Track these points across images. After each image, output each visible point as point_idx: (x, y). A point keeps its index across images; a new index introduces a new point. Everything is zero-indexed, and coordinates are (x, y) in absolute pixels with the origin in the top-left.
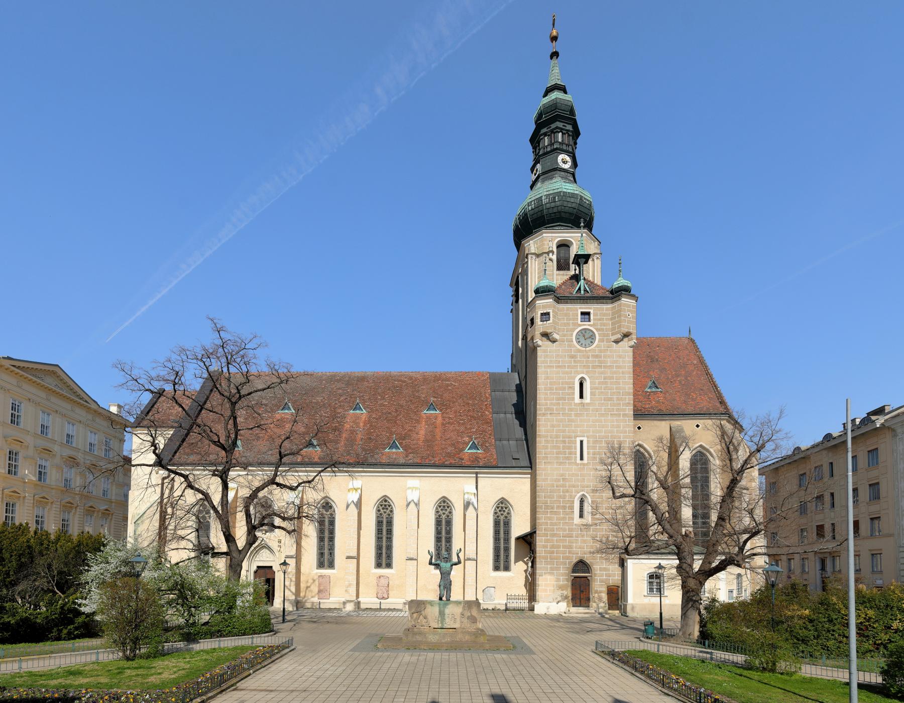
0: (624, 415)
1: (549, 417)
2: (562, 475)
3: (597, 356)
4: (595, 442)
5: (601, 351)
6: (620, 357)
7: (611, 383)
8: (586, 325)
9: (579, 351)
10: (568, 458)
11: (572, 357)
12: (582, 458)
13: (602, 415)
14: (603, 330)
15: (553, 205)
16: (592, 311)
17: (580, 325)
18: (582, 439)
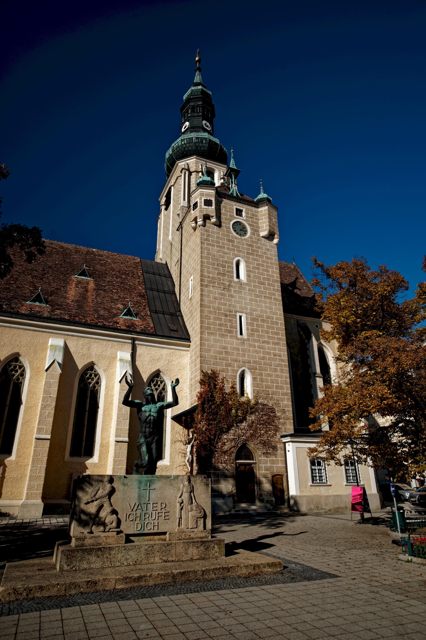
0: (275, 299)
1: (211, 289)
2: (224, 348)
3: (250, 245)
4: (253, 319)
5: (253, 242)
6: (268, 250)
9: (236, 238)
10: (230, 332)
11: (229, 241)
13: (258, 296)
14: (253, 226)
15: (201, 145)
16: (244, 210)
17: (236, 218)
18: (241, 314)
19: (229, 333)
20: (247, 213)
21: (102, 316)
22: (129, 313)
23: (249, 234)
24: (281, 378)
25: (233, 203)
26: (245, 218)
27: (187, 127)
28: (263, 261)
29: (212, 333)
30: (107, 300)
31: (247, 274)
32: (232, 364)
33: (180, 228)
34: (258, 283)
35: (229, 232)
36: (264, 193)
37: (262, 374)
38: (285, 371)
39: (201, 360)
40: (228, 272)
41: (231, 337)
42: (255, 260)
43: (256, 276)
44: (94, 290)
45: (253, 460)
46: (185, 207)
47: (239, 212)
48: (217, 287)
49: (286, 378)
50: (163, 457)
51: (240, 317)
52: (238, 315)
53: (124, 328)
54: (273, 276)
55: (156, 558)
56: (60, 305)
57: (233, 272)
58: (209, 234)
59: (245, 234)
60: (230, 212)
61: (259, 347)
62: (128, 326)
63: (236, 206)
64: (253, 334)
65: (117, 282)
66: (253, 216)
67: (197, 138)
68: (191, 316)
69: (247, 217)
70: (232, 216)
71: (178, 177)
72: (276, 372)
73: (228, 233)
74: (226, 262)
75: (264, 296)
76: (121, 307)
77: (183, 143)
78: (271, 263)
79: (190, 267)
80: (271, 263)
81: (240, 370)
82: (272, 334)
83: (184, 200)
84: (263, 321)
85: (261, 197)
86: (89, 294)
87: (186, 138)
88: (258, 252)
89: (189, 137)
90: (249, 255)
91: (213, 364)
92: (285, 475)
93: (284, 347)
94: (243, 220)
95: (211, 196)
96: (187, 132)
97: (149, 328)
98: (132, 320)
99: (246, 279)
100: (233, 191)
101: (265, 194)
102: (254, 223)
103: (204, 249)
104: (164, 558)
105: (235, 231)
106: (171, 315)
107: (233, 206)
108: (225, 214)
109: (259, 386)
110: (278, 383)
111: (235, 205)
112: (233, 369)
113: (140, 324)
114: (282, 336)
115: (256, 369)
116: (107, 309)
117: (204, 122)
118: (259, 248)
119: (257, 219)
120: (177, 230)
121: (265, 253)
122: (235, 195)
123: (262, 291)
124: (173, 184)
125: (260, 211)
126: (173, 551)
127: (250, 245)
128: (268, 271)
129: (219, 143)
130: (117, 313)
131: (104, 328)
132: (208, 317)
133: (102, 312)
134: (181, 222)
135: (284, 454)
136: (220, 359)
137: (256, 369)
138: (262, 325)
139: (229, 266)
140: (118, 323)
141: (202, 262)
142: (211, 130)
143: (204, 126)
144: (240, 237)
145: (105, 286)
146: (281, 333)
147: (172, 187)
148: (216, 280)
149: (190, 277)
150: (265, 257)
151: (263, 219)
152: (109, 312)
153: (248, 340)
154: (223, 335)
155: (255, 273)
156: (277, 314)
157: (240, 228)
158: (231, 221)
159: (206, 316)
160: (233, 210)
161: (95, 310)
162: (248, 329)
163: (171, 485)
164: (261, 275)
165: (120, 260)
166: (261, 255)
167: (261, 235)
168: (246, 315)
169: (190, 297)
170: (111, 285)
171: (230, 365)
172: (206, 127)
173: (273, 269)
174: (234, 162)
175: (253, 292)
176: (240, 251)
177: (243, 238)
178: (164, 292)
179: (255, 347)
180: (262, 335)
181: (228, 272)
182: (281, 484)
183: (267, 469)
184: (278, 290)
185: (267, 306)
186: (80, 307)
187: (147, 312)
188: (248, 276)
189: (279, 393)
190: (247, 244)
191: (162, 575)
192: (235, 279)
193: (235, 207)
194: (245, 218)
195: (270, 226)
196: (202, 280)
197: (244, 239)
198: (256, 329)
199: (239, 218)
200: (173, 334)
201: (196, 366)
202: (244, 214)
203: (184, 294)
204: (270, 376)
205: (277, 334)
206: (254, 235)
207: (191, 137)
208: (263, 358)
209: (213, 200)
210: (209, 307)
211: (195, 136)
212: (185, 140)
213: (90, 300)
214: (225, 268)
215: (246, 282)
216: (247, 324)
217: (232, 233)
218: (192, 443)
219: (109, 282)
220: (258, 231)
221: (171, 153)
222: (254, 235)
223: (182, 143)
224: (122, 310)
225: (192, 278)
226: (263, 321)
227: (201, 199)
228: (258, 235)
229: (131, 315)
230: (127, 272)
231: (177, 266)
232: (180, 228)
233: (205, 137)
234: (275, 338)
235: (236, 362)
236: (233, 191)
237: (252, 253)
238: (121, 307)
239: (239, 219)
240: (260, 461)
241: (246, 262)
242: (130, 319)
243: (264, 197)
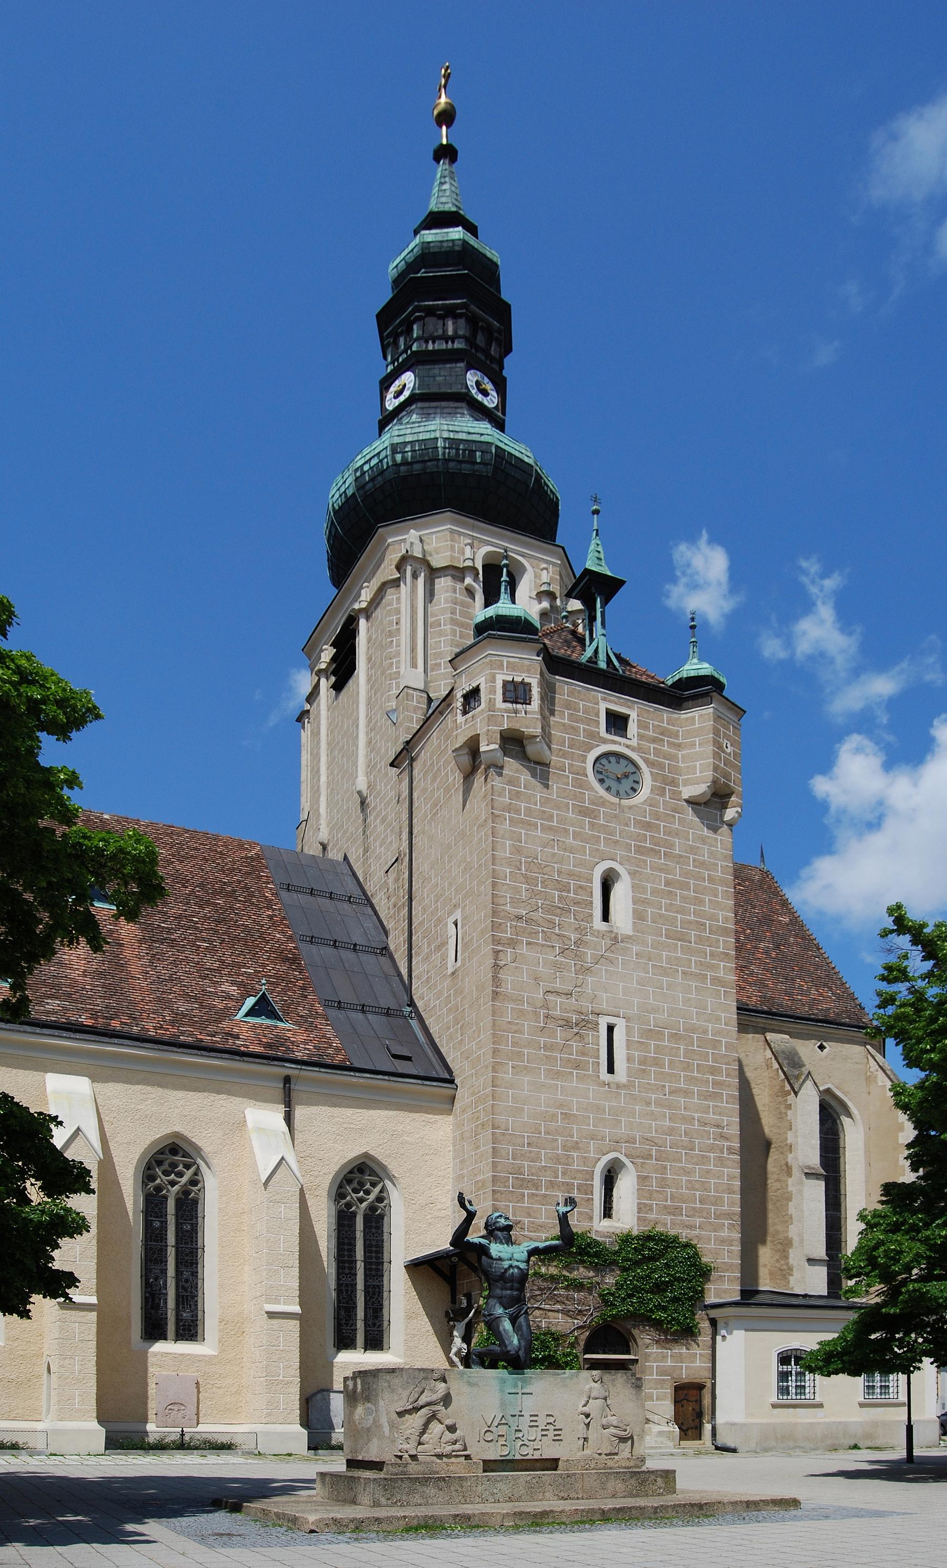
3: (648, 826)
5: (657, 816)
8: (617, 744)
9: (603, 803)
11: (584, 812)
12: (611, 1070)
14: (661, 766)
16: (633, 716)
17: (605, 741)
18: (612, 1020)
19: (577, 1067)
20: (642, 725)
23: (645, 792)
25: (598, 693)
26: (634, 742)
28: (686, 874)
29: (526, 1068)
31: (635, 911)
35: (581, 784)
36: (701, 660)
40: (577, 903)
42: (661, 870)
43: (661, 916)
47: (617, 723)
51: (611, 1029)
52: (603, 1022)
57: (592, 903)
59: (634, 790)
60: (589, 721)
63: (605, 701)
64: (644, 1070)
66: (662, 734)
69: (641, 737)
73: (581, 787)
74: (571, 874)
85: (693, 674)
88: (671, 846)
90: (642, 854)
91: (529, 1144)
94: (628, 746)
99: (630, 926)
100: (596, 651)
101: (706, 665)
105: (601, 781)
107: (598, 704)
108: (573, 727)
111: (604, 699)
119: (674, 744)
122: (603, 665)
125: (687, 719)
148: (539, 925)
150: (694, 861)
151: (693, 745)
154: (558, 1072)
157: (618, 773)
160: (597, 715)
162: (629, 1059)
171: (576, 1146)
175: (649, 959)
176: (617, 841)
177: (625, 802)
179: (648, 1104)
180: (670, 1075)
181: (577, 903)
188: (639, 916)
190: (637, 822)
192: (598, 923)
193: (603, 707)
194: (634, 742)
195: (716, 769)
198: (655, 1058)
199: (614, 742)
202: (632, 728)
208: (671, 1131)
214: (569, 892)
217: (591, 789)
236: (596, 651)
239: (617, 744)
241: (632, 874)
243: (702, 673)
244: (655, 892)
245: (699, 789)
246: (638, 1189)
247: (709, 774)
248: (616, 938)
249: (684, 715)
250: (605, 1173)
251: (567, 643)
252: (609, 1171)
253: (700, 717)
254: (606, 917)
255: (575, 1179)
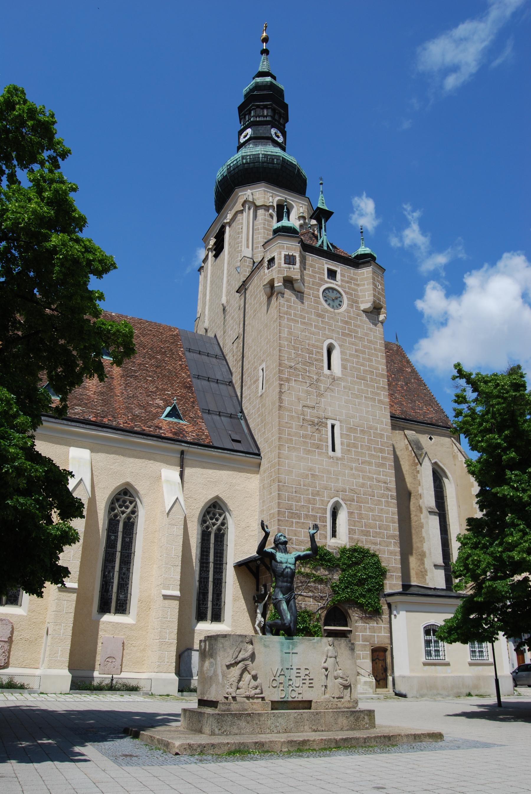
0: (380, 401)
1: (293, 384)
2: (310, 470)
3: (346, 323)
4: (350, 429)
7: (364, 359)
8: (332, 284)
9: (327, 311)
11: (319, 315)
12: (334, 450)
14: (351, 294)
16: (339, 271)
17: (327, 282)
18: (334, 422)
19: (318, 448)
20: (342, 275)
21: (138, 416)
22: (174, 413)
23: (345, 306)
24: (387, 513)
25: (324, 261)
26: (339, 283)
27: (248, 137)
28: (364, 346)
29: (294, 448)
30: (140, 393)
31: (342, 365)
32: (320, 493)
33: (242, 289)
34: (357, 378)
35: (318, 302)
36: (366, 246)
37: (361, 507)
38: (392, 505)
39: (279, 485)
40: (317, 360)
41: (320, 454)
42: (353, 344)
43: (354, 367)
44: (121, 377)
45: (346, 625)
46: (248, 258)
47: (332, 274)
48: (302, 382)
49: (393, 514)
50: (222, 620)
51: (333, 427)
52: (330, 423)
53: (170, 435)
54: (377, 369)
55: (306, 727)
56: (79, 399)
57: (323, 360)
58: (291, 305)
59: (340, 305)
60: (320, 273)
61: (357, 469)
62: (175, 434)
63: (327, 264)
64: (349, 450)
65: (152, 365)
66: (351, 279)
67: (266, 156)
68: (262, 421)
69: (342, 281)
70: (322, 280)
71: (237, 213)
72: (379, 505)
73: (317, 303)
74: (313, 346)
75: (365, 397)
76: (161, 403)
77: (244, 161)
78: (375, 349)
79: (261, 350)
80: (375, 349)
81: (332, 501)
82: (374, 451)
83: (248, 247)
84: (363, 432)
85: (363, 253)
86: (115, 382)
87: (249, 154)
89: (253, 153)
90: (344, 336)
91: (295, 492)
92: (389, 649)
93: (392, 470)
94: (337, 285)
95: (295, 250)
96: (249, 144)
97: (203, 437)
98: (179, 423)
99: (340, 372)
100: (323, 242)
101: (368, 249)
102: (352, 290)
103: (284, 327)
104: (314, 727)
105: (326, 301)
106: (231, 416)
107: (323, 265)
108: (313, 276)
109: (357, 524)
110: (381, 521)
111: (326, 263)
112: (322, 500)
113: (190, 429)
114: (388, 454)
115: (353, 500)
116: (144, 407)
117: (273, 131)
118: (359, 327)
120: (237, 292)
121: (367, 334)
122: (325, 248)
123: (362, 389)
124: (228, 221)
125: (361, 273)
126: (322, 721)
127: (346, 323)
128: (370, 360)
129: (295, 163)
130: (157, 413)
131: (142, 434)
132: (289, 425)
133: (137, 411)
134: (244, 282)
135: (388, 620)
136: (304, 485)
137: (353, 500)
138: (362, 438)
139: (318, 352)
140: (160, 428)
141: (280, 345)
142: (282, 142)
143: (274, 136)
144: (332, 310)
145: (135, 371)
146: (388, 450)
147: (227, 228)
148: (300, 371)
149: (260, 365)
150: (367, 340)
151: (364, 285)
152: (146, 412)
153: (342, 459)
154: (309, 450)
155: (353, 364)
156: (382, 422)
157: (333, 297)
158: (321, 285)
159: (286, 423)
160: (324, 270)
161: (127, 408)
162: (342, 444)
163: (315, 648)
164: (361, 365)
165: (150, 330)
166: (361, 338)
167: (362, 308)
168: (340, 423)
169: (260, 394)
170: (144, 370)
171: (318, 494)
172: (276, 138)
173: (378, 358)
174: (323, 199)
175: (350, 390)
176: (333, 330)
177: (336, 311)
178: (217, 381)
179: (352, 469)
180: (361, 452)
181: (317, 360)
182: (383, 660)
183: (365, 640)
184: (384, 388)
185: (368, 411)
186: (106, 402)
187: (197, 412)
188: (344, 367)
189: (384, 535)
190: (342, 320)
191: (325, 740)
192: (326, 371)
193: (326, 267)
194: (339, 283)
195: (374, 296)
196: (280, 371)
197: (339, 314)
198: (354, 443)
199: (331, 283)
200: (236, 446)
201: (271, 493)
202: (338, 276)
203: (249, 387)
204: (372, 510)
205: (382, 451)
206: (352, 307)
207: (256, 153)
208: (363, 485)
209: (297, 255)
210: (290, 411)
211: (263, 152)
212: (248, 157)
213: (118, 391)
214: (313, 354)
215: (341, 376)
216: (342, 435)
217: (322, 304)
218: (264, 602)
219: (140, 365)
220: (357, 302)
221: (225, 174)
222: (352, 307)
223: (242, 162)
224: (162, 409)
225: (264, 365)
226: (363, 432)
227: (280, 254)
228: (358, 308)
229: (178, 417)
230: (163, 350)
231: (235, 344)
232: (242, 289)
233: (277, 154)
234: (379, 457)
235: (326, 489)
236: (323, 242)
237: (349, 334)
238: (161, 403)
239: (332, 284)
240: (357, 627)
241: (340, 346)
242: (175, 423)
243: (366, 252)
244: (351, 355)
245: (367, 305)
246: (349, 520)
247: (371, 298)
248: (334, 379)
249: (360, 271)
250: (332, 510)
251: (311, 238)
252: (334, 509)
253: (367, 272)
254: (329, 368)
255: (317, 513)
